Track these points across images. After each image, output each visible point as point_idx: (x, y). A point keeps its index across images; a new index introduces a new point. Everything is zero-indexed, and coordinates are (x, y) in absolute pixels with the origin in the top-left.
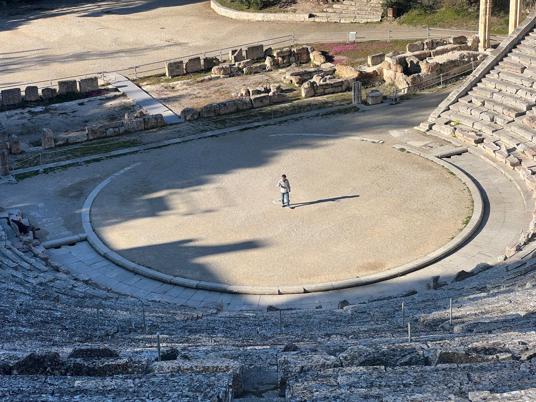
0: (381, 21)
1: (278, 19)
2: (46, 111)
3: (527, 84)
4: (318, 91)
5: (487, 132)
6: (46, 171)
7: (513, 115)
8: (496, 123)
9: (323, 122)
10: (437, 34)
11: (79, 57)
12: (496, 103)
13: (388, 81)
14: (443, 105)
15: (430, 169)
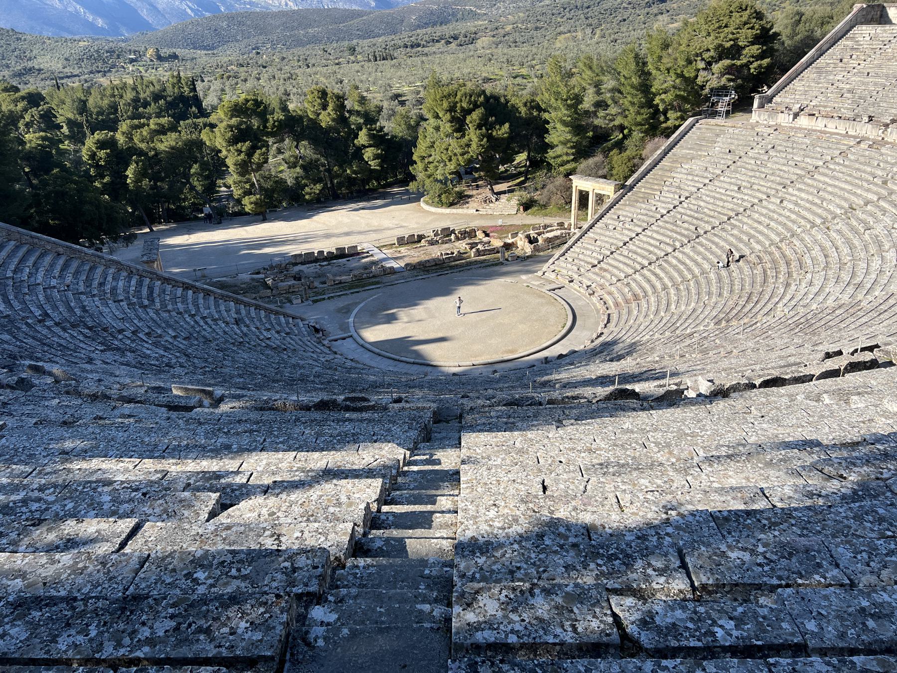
2: (329, 264)
3: (598, 249)
5: (575, 276)
6: (329, 298)
9: (483, 271)
10: (548, 221)
11: (347, 234)
12: (580, 260)
13: (520, 248)
14: (551, 261)
15: (543, 297)
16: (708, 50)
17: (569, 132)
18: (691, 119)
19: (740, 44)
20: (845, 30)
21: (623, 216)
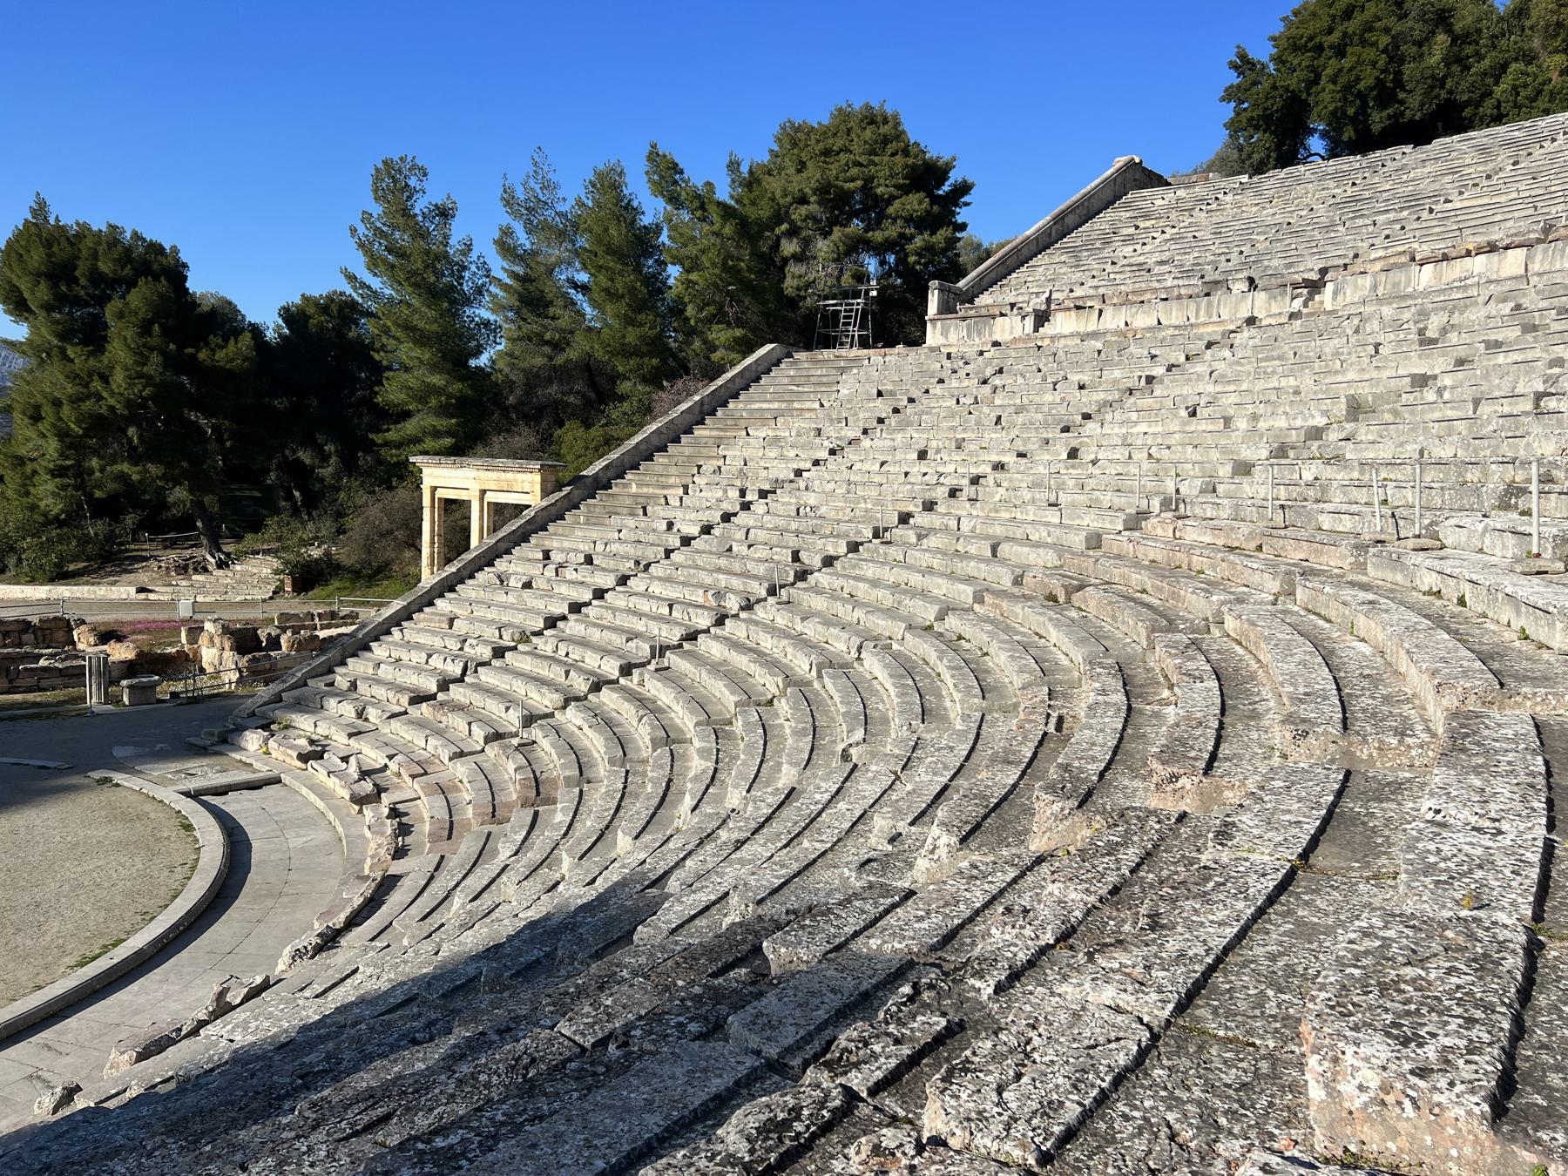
0: (271, 598)
1: (78, 595)
4: (19, 683)
5: (340, 739)
7: (405, 700)
8: (366, 720)
12: (379, 682)
16: (803, 200)
17: (434, 368)
18: (769, 347)
19: (879, 191)
20: (1096, 204)
21: (562, 550)
